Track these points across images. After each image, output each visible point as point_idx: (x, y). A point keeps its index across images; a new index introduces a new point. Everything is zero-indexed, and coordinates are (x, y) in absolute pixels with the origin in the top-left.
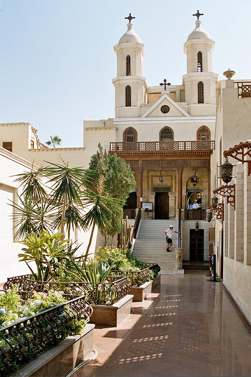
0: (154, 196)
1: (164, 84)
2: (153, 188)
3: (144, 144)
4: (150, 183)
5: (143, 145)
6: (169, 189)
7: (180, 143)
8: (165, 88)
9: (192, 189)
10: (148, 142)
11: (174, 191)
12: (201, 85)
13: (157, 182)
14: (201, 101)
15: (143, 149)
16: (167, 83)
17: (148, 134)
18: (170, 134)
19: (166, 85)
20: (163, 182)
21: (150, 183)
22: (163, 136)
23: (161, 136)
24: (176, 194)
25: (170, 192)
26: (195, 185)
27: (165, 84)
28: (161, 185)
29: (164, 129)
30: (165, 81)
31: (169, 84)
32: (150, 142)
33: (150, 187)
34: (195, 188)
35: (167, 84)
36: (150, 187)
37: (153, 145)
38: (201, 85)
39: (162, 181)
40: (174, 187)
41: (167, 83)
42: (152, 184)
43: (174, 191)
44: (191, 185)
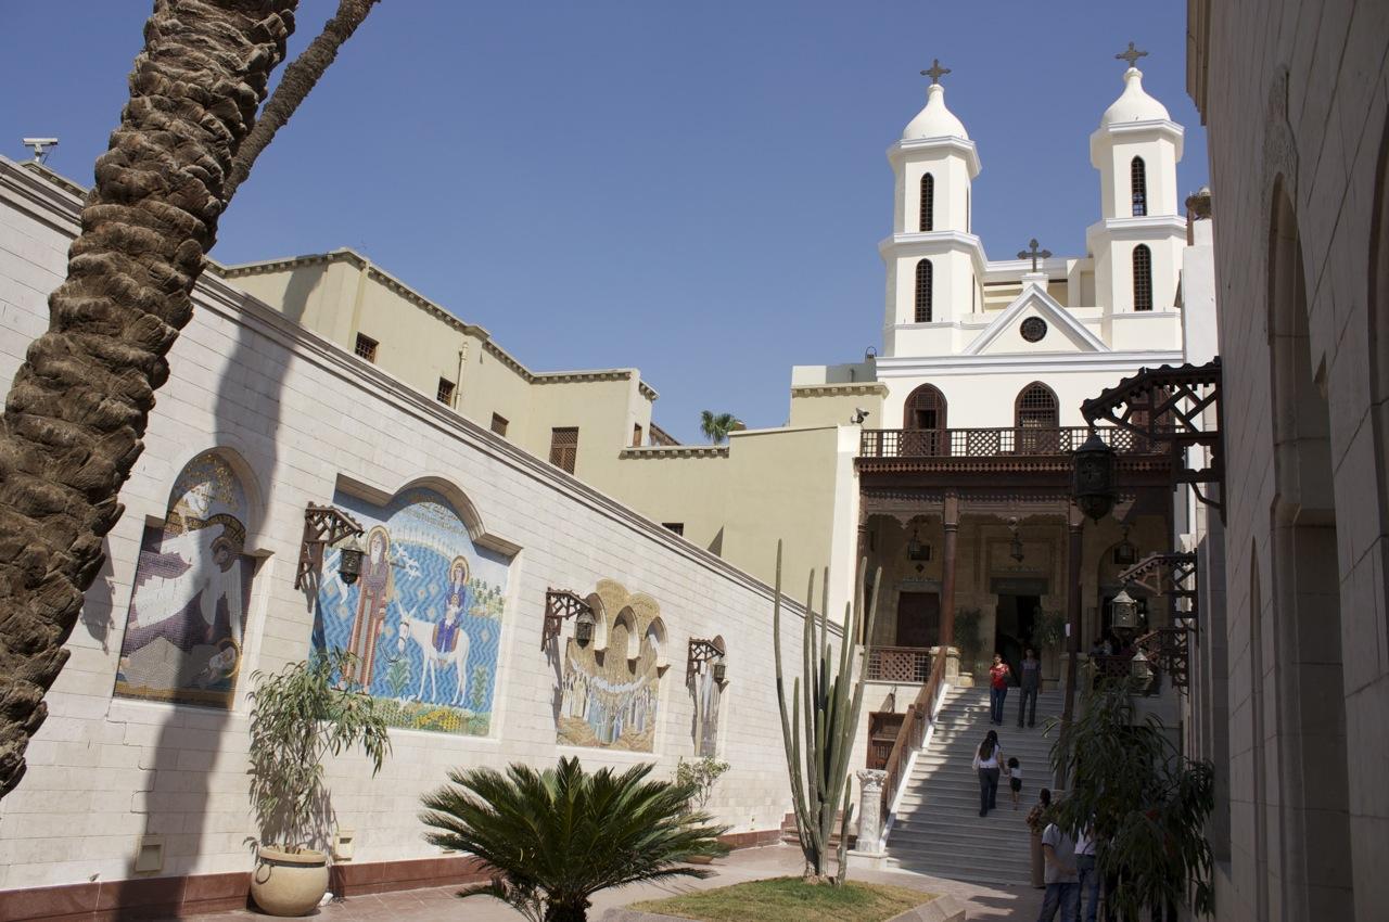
2: (993, 579)
3: (964, 434)
4: (983, 564)
6: (1044, 583)
7: (1074, 433)
10: (976, 431)
11: (1057, 591)
14: (1143, 303)
17: (981, 409)
18: (1049, 405)
20: (1023, 561)
21: (983, 564)
22: (1025, 412)
23: (1021, 412)
25: (1046, 593)
29: (1030, 392)
30: (1034, 244)
32: (984, 431)
33: (982, 575)
36: (982, 575)
37: (991, 438)
39: (1020, 559)
41: (1039, 250)
43: (1057, 591)
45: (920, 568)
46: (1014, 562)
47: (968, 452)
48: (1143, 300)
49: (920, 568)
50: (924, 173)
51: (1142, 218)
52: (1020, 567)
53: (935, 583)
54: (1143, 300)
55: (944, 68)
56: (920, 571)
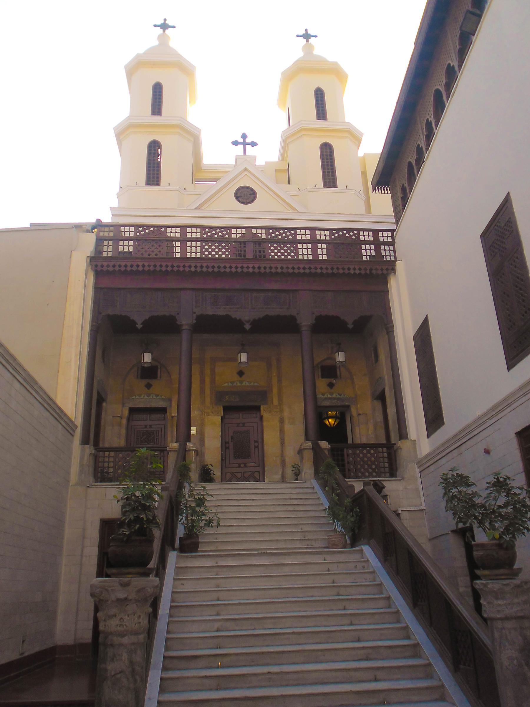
0: (218, 419)
1: (240, 143)
4: (208, 380)
5: (196, 247)
8: (245, 153)
9: (326, 396)
11: (275, 401)
12: (327, 153)
13: (226, 377)
15: (196, 253)
16: (248, 140)
19: (247, 146)
21: (208, 380)
24: (282, 411)
26: (331, 385)
27: (244, 144)
28: (239, 384)
30: (244, 136)
31: (254, 144)
33: (208, 391)
34: (332, 394)
35: (248, 144)
36: (208, 391)
38: (327, 153)
40: (275, 390)
41: (248, 140)
42: (213, 381)
44: (322, 384)
45: (149, 386)
46: (236, 377)
47: (202, 253)
48: (330, 178)
49: (149, 386)
50: (153, 83)
51: (322, 124)
52: (241, 382)
53: (163, 400)
54: (330, 178)
55: (170, 24)
56: (149, 389)
